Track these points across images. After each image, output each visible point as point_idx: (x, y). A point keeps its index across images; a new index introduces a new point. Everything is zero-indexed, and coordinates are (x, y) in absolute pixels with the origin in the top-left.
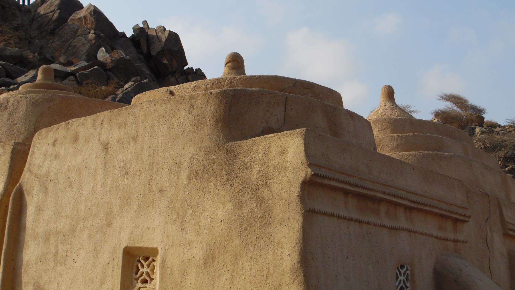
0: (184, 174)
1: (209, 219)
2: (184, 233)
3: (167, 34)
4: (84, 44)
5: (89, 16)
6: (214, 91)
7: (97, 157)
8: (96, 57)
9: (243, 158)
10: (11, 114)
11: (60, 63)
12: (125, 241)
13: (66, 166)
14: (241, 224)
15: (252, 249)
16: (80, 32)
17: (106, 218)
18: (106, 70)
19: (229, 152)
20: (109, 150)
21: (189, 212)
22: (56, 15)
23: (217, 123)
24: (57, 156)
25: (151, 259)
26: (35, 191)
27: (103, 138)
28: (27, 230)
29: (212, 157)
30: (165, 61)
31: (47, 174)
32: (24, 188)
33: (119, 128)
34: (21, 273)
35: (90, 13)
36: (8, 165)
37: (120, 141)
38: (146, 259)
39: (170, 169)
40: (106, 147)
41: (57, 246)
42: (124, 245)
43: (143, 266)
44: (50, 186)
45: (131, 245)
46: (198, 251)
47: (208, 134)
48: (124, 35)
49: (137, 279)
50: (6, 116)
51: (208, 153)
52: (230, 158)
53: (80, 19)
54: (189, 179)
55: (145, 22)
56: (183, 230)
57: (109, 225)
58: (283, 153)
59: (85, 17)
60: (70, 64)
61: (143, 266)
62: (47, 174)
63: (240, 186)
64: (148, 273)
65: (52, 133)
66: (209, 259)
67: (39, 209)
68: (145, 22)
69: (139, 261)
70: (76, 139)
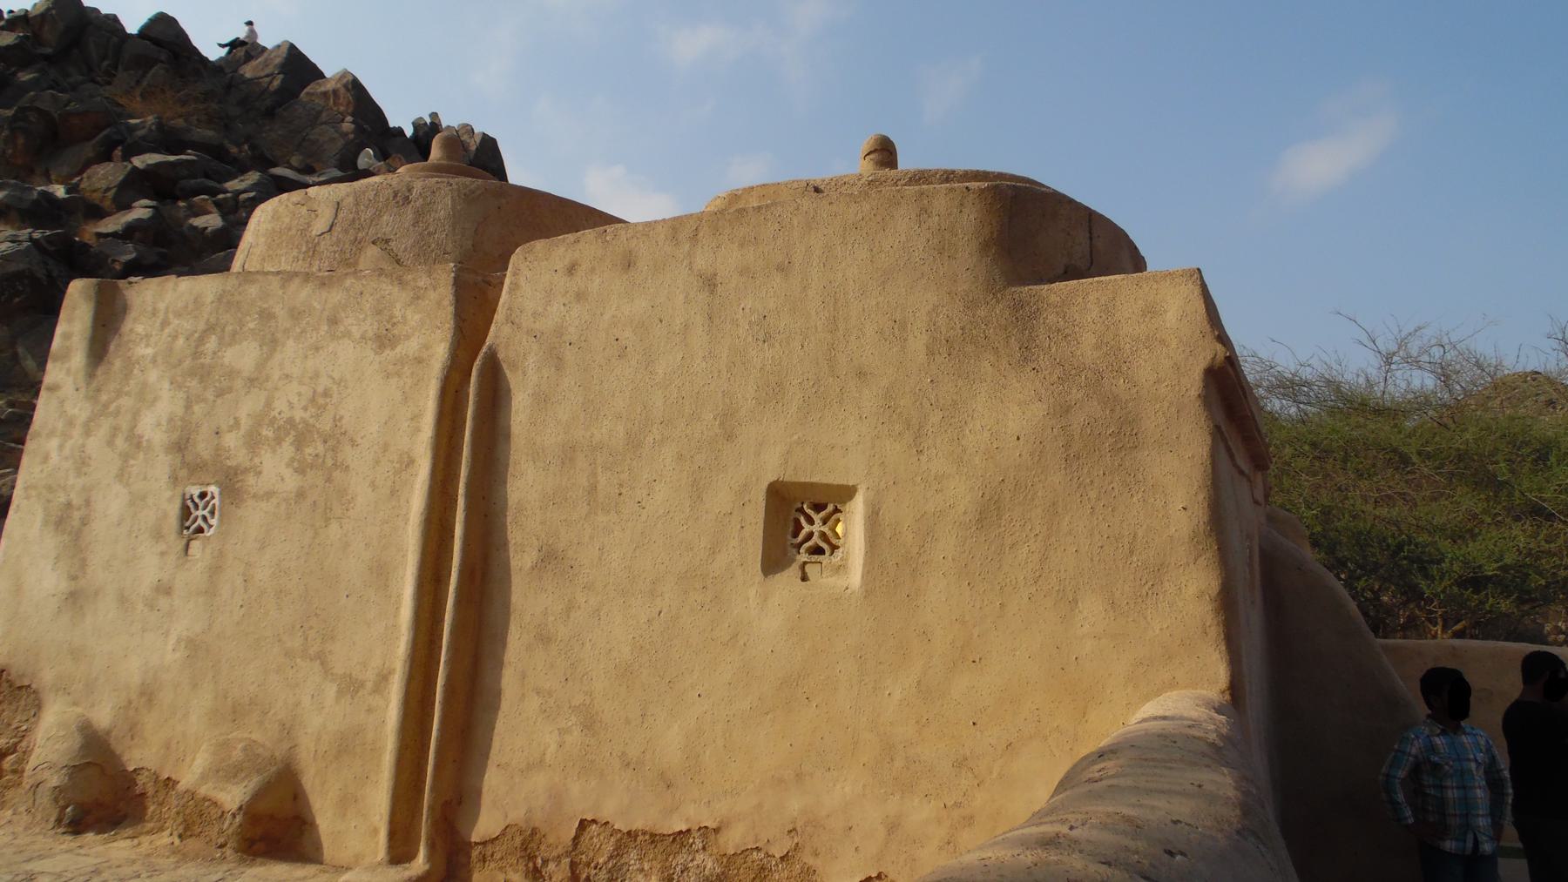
0: (918, 343)
1: (986, 434)
2: (924, 458)
3: (478, 139)
4: (333, 140)
5: (343, 91)
6: (974, 185)
7: (687, 301)
8: (355, 164)
9: (1052, 319)
10: (419, 214)
11: (291, 167)
12: (773, 470)
13: (606, 317)
14: (1067, 446)
15: (1093, 494)
16: (324, 117)
17: (722, 424)
19: (1018, 306)
20: (719, 288)
21: (935, 418)
22: (276, 83)
23: (985, 247)
24: (580, 296)
25: (830, 508)
26: (531, 361)
27: (701, 262)
29: (981, 312)
31: (559, 331)
32: (501, 356)
33: (742, 245)
34: (505, 525)
35: (345, 86)
36: (451, 309)
37: (744, 271)
38: (818, 508)
39: (880, 332)
40: (710, 283)
41: (594, 474)
43: (811, 521)
44: (569, 355)
45: (789, 477)
46: (961, 495)
47: (967, 264)
48: (400, 131)
49: (800, 545)
51: (971, 305)
52: (1023, 317)
53: (325, 94)
54: (931, 353)
55: (434, 115)
56: (920, 452)
57: (730, 437)
58: (1151, 311)
59: (335, 92)
61: (811, 521)
62: (559, 331)
63: (1058, 371)
64: (823, 536)
65: (562, 249)
67: (542, 400)
68: (434, 115)
69: (801, 510)
70: (628, 263)
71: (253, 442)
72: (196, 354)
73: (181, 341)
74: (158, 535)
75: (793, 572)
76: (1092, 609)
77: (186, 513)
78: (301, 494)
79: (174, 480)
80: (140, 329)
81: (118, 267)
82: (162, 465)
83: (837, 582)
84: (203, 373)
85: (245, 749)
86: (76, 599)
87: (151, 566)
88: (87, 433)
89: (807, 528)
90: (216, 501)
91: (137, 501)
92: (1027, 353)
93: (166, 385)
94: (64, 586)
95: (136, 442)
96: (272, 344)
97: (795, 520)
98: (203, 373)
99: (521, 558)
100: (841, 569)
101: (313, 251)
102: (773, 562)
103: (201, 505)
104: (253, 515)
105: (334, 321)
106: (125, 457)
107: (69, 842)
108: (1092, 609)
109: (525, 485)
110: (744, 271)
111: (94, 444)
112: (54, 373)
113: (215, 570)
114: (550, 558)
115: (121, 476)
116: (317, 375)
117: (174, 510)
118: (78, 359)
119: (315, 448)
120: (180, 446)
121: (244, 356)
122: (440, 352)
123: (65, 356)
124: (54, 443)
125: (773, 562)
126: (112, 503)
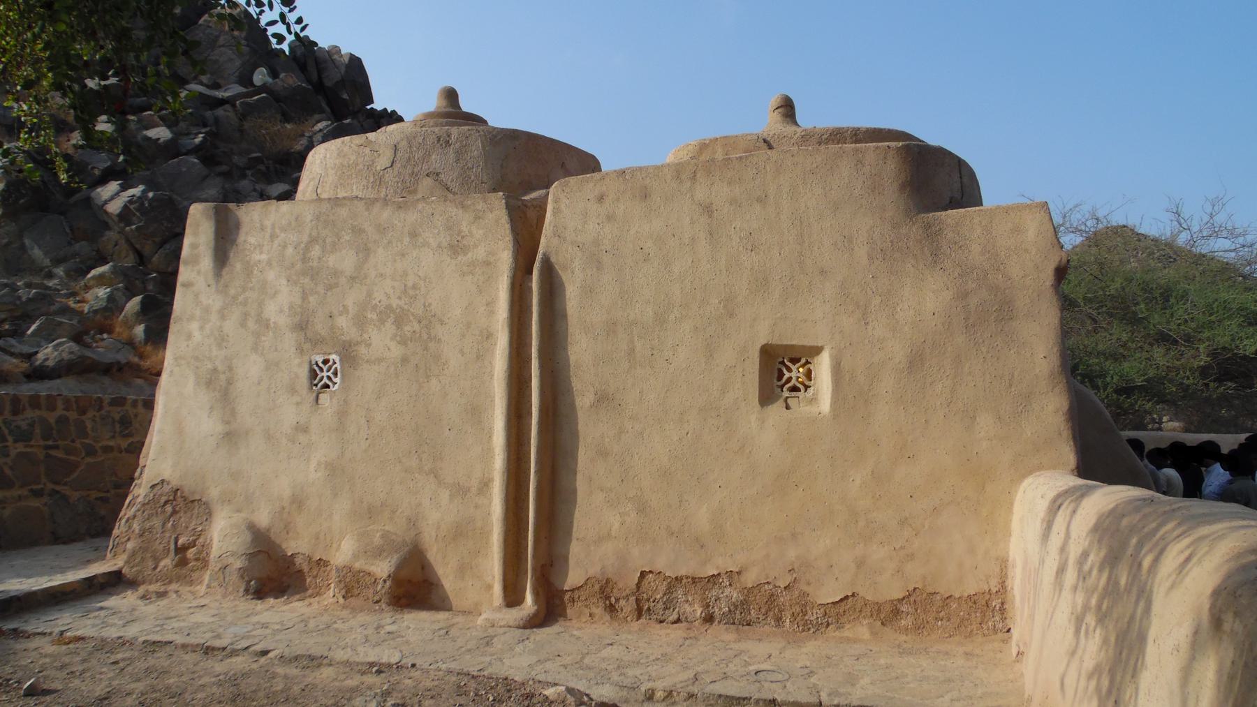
0: (862, 252)
1: (912, 312)
2: (870, 327)
3: (347, 60)
4: (230, 60)
6: (892, 144)
7: (692, 222)
9: (950, 235)
11: (201, 83)
13: (632, 232)
14: (966, 319)
15: (984, 349)
16: (221, 41)
17: (725, 306)
18: (278, 100)
19: (928, 226)
20: (715, 214)
21: (876, 301)
23: (903, 187)
24: (610, 218)
25: (803, 361)
26: (577, 264)
27: (701, 193)
28: (569, 318)
29: (903, 231)
30: (345, 96)
32: (553, 259)
33: (729, 183)
34: (569, 377)
36: (508, 226)
37: (733, 202)
38: (795, 361)
39: (835, 244)
40: (708, 210)
41: (632, 342)
42: (763, 342)
43: (790, 370)
45: (776, 341)
46: (898, 351)
47: (891, 197)
49: (782, 387)
50: (452, 155)
52: (931, 234)
54: (871, 258)
56: (867, 324)
60: (217, 86)
61: (790, 370)
62: (597, 242)
63: (958, 270)
65: (591, 185)
66: (915, 362)
67: (588, 291)
69: (783, 363)
71: (360, 322)
72: (305, 260)
73: (290, 250)
74: (292, 390)
75: (780, 404)
76: (985, 422)
77: (313, 375)
78: (405, 360)
79: (300, 350)
80: (252, 240)
81: (97, 172)
82: (289, 341)
83: (813, 410)
84: (313, 274)
85: (382, 537)
86: (231, 438)
87: (289, 413)
88: (223, 317)
89: (787, 375)
90: (338, 365)
91: (272, 366)
92: (936, 257)
93: (284, 282)
94: (220, 428)
95: (265, 324)
96: (365, 251)
97: (779, 370)
98: (313, 274)
99: (583, 399)
100: (813, 400)
101: (379, 181)
102: (766, 398)
103: (325, 368)
104: (368, 376)
105: (414, 235)
106: (257, 335)
107: (260, 605)
108: (985, 422)
109: (581, 349)
110: (733, 202)
111: (230, 326)
112: (185, 274)
113: (342, 414)
114: (603, 399)
115: (255, 348)
116: (405, 274)
117: (304, 373)
118: (207, 263)
119: (411, 327)
120: (301, 326)
121: (345, 260)
122: (505, 258)
123: (195, 260)
124: (194, 326)
125: (766, 398)
126: (251, 368)
